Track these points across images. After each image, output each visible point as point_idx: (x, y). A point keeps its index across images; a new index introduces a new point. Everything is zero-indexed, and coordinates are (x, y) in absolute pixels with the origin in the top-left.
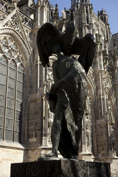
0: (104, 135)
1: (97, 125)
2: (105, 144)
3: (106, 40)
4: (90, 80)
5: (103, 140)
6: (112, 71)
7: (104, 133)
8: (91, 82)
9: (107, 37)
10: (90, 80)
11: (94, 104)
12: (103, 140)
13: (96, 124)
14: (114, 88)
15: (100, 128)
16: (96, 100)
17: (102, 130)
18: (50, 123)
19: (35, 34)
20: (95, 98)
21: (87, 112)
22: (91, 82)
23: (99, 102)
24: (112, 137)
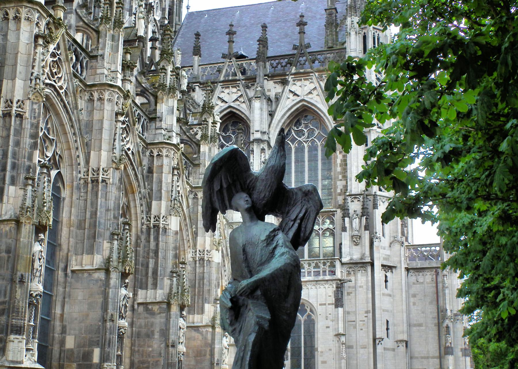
0: (157, 336)
1: (139, 304)
2: (157, 361)
3: (166, 22)
4: (134, 169)
5: (150, 349)
6: (194, 146)
7: (157, 329)
8: (136, 174)
9: (171, 13)
10: (134, 169)
11: (137, 240)
12: (150, 349)
13: (135, 303)
14: (192, 196)
15: (148, 316)
16: (144, 230)
17: (153, 320)
18: (34, 295)
19: (7, 14)
20: (142, 224)
21: (127, 268)
22: (136, 174)
23: (152, 237)
24: (179, 343)
